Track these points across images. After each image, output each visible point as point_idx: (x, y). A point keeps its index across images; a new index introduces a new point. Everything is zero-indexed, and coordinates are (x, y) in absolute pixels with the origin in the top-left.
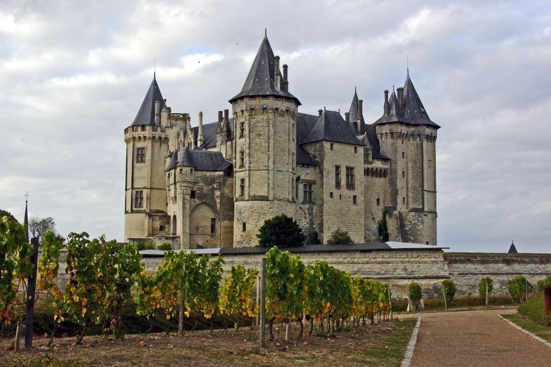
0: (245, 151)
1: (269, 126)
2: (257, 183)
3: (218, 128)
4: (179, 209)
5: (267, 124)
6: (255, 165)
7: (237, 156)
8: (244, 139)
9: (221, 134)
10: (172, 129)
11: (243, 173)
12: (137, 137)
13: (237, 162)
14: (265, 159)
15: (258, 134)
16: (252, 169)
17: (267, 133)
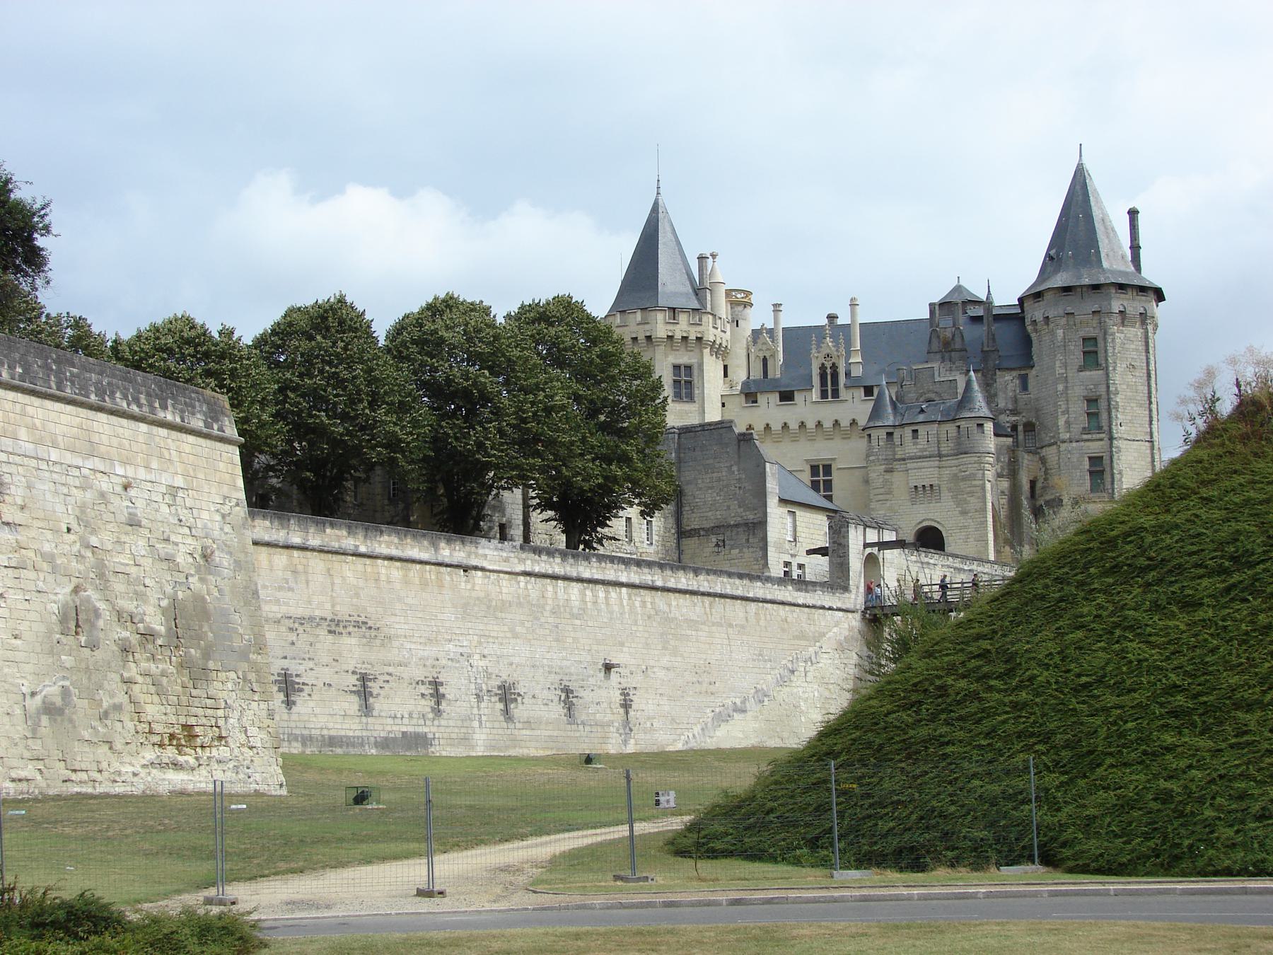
0: (1103, 397)
1: (1147, 351)
2: (1134, 466)
3: (935, 341)
4: (964, 513)
5: (1144, 347)
6: (1128, 428)
7: (1070, 406)
8: (1101, 372)
9: (947, 355)
10: (737, 326)
11: (1101, 443)
12: (678, 335)
13: (1072, 420)
14: (1144, 419)
15: (1130, 364)
16: (1125, 436)
17: (1145, 364)
